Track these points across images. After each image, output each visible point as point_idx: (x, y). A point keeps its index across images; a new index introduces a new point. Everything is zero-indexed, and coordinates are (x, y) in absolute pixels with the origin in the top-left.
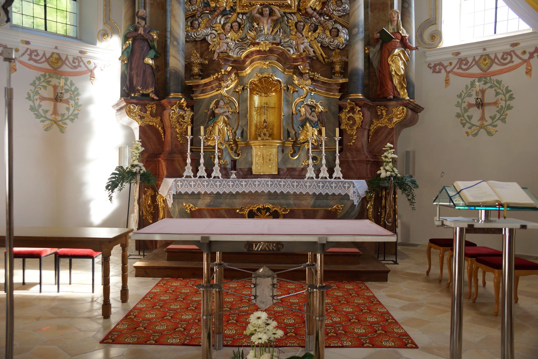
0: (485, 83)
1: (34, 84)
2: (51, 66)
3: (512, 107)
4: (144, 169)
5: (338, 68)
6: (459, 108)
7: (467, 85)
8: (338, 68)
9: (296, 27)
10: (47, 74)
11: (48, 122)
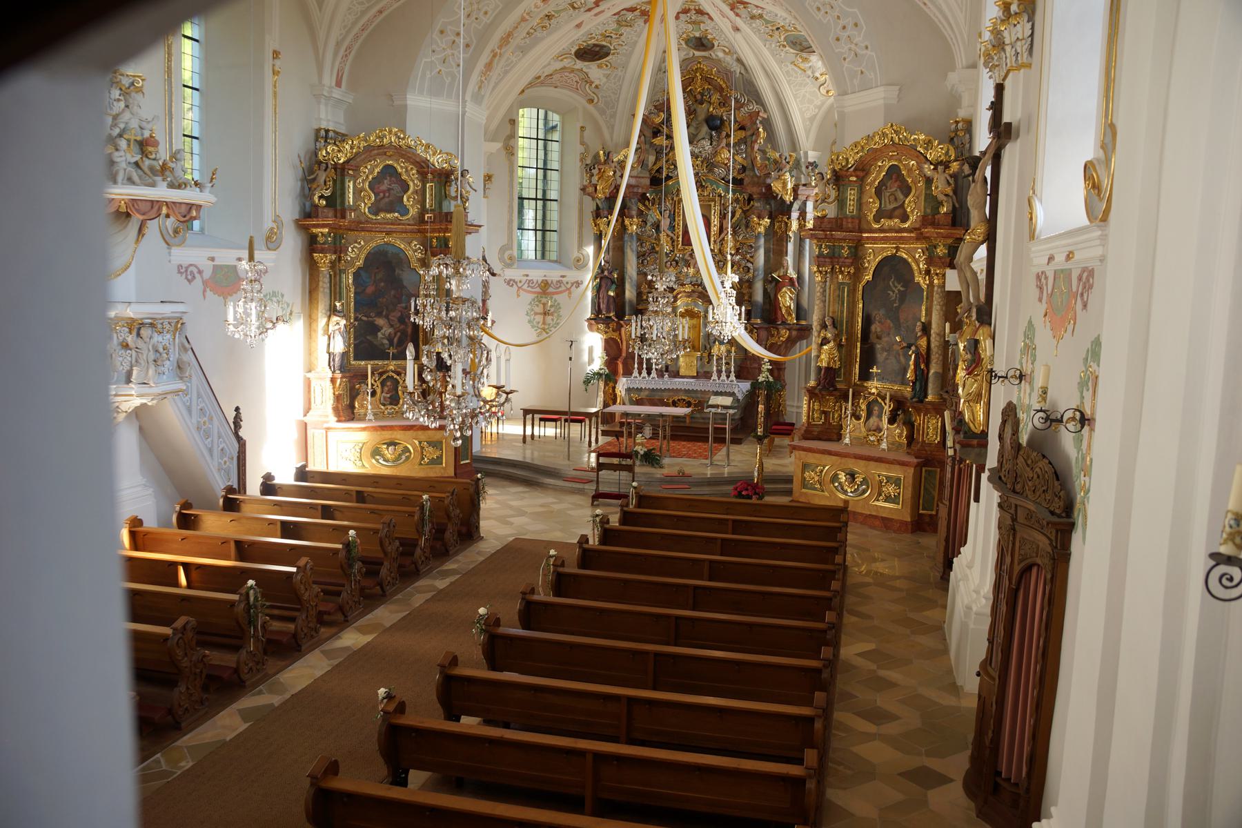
4: (607, 371)
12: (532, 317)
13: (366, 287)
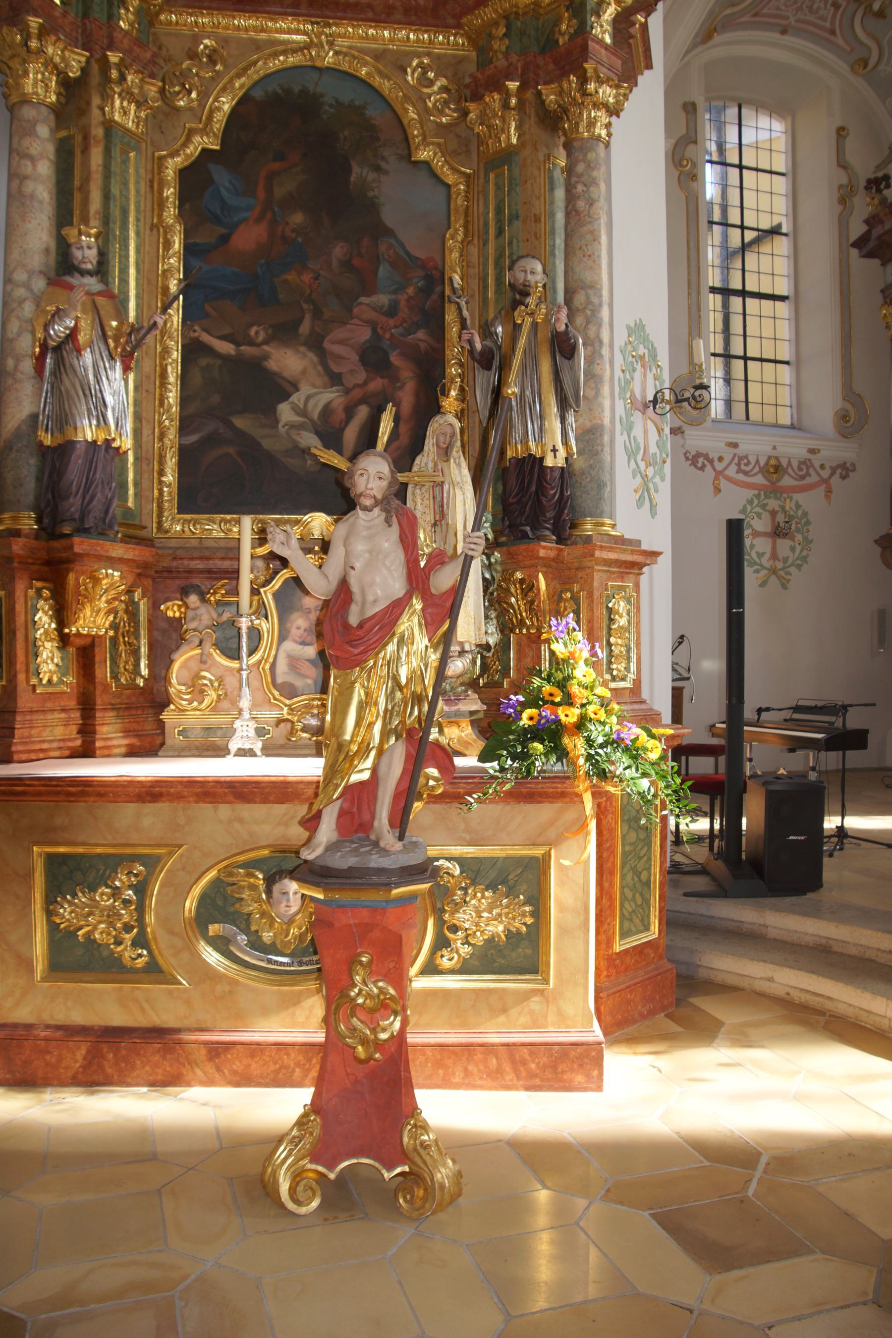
2: (767, 480)
10: (762, 492)
11: (764, 572)
13: (234, 227)
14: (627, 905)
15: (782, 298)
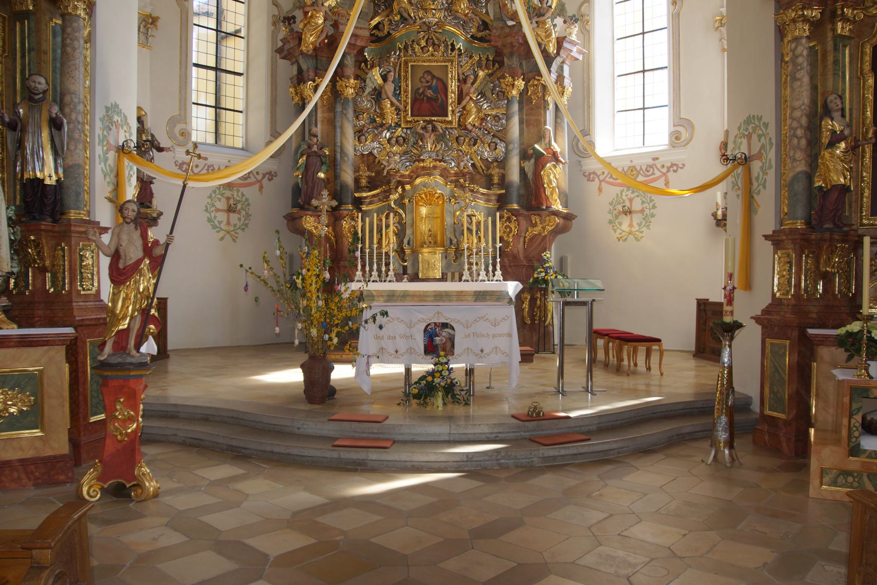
0: (633, 192)
1: (210, 197)
3: (655, 215)
5: (496, 180)
6: (611, 215)
7: (617, 194)
8: (496, 180)
9: (457, 141)
12: (213, 214)
14: (94, 400)
15: (240, 74)
